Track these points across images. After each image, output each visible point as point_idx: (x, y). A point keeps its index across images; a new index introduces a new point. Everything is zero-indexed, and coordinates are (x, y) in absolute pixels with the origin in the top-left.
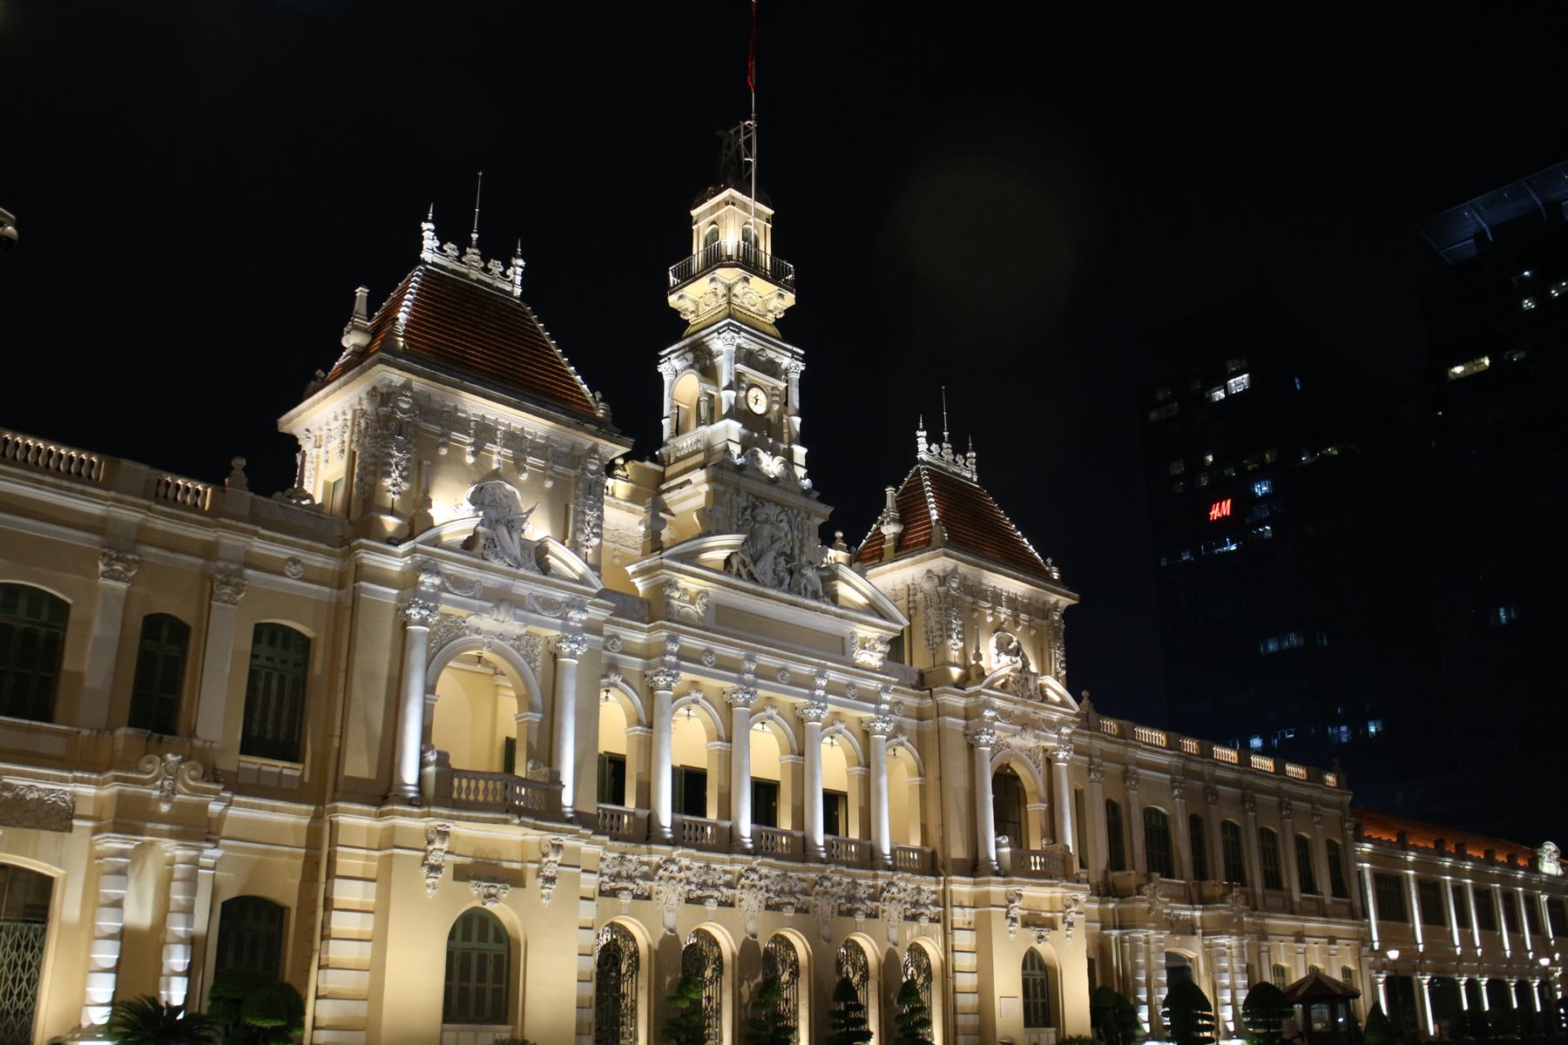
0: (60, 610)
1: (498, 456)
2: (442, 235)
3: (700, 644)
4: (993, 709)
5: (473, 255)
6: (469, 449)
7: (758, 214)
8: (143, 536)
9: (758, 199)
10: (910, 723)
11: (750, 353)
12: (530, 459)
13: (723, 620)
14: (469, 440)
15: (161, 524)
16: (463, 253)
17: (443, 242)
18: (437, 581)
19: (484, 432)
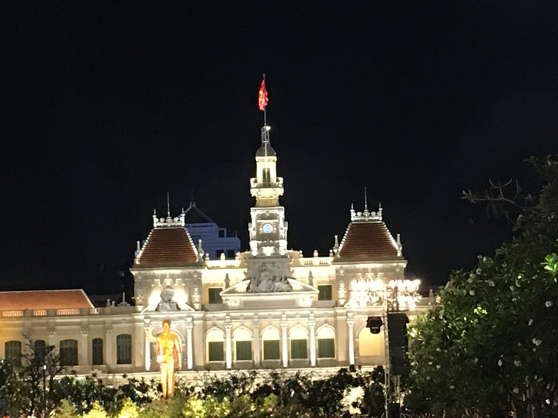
0: (76, 342)
1: (168, 282)
2: (159, 217)
3: (239, 314)
4: (352, 312)
5: (169, 219)
6: (160, 282)
7: (269, 161)
8: (89, 323)
9: (268, 155)
10: (331, 319)
11: (263, 214)
12: (177, 279)
13: (246, 306)
14: (159, 280)
15: (92, 320)
16: (166, 219)
17: (159, 219)
18: (149, 320)
19: (163, 277)
